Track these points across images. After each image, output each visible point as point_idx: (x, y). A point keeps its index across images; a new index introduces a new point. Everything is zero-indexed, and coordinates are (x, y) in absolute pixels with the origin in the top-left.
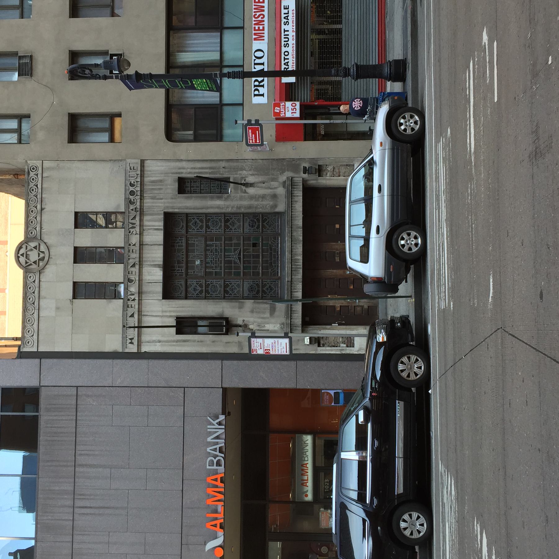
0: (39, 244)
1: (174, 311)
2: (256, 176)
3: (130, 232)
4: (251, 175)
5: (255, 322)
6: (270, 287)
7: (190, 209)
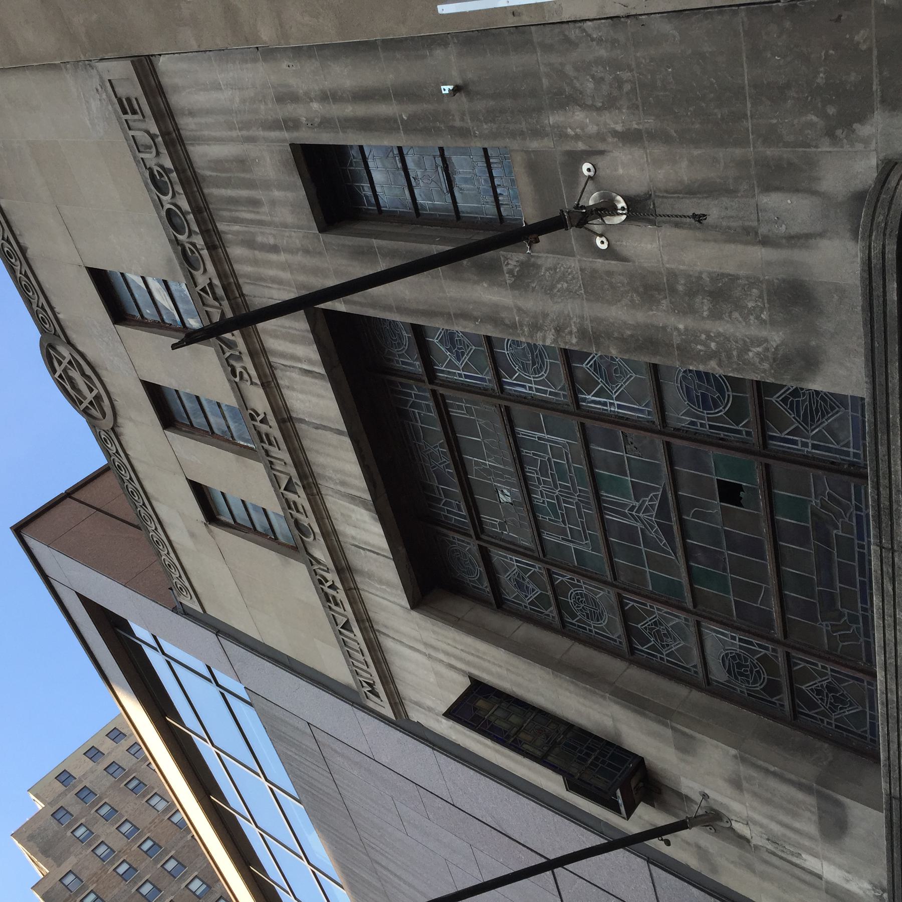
2: (658, 150)
4: (630, 137)
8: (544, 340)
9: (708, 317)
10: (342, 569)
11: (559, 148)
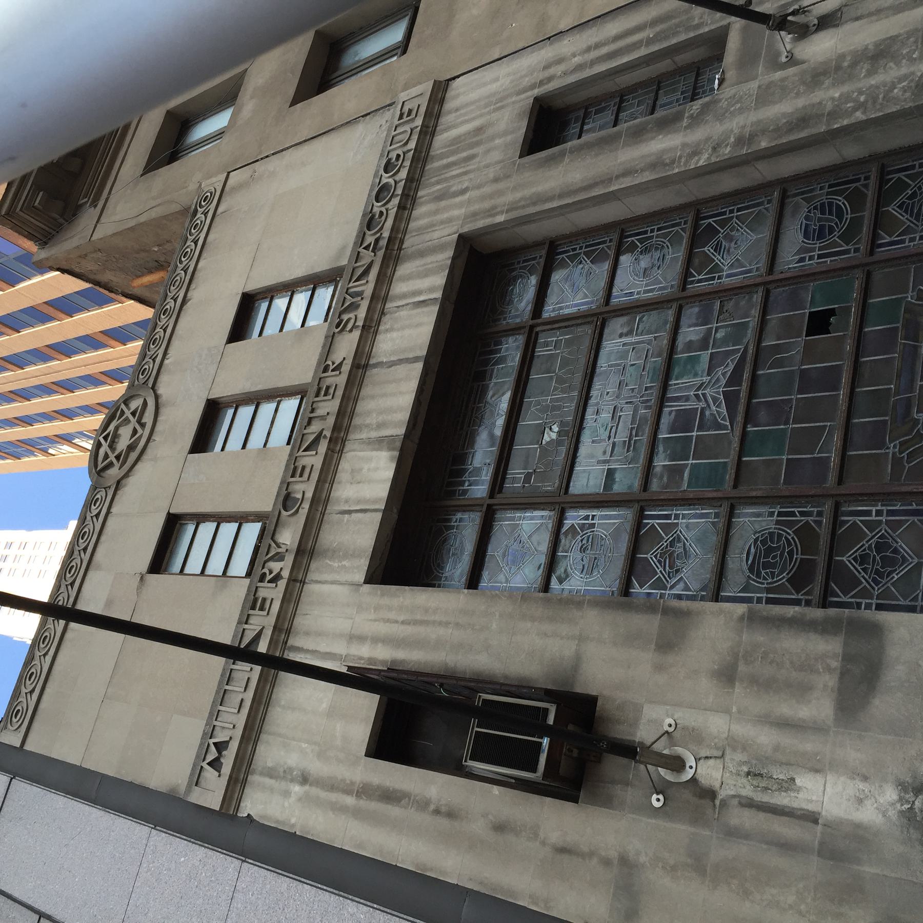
0: (145, 404)
1: (386, 640)
3: (337, 327)
5: (733, 743)
6: (880, 547)
7: (551, 199)
8: (697, 162)
9: (865, 77)
10: (304, 552)
11: (776, 5)
